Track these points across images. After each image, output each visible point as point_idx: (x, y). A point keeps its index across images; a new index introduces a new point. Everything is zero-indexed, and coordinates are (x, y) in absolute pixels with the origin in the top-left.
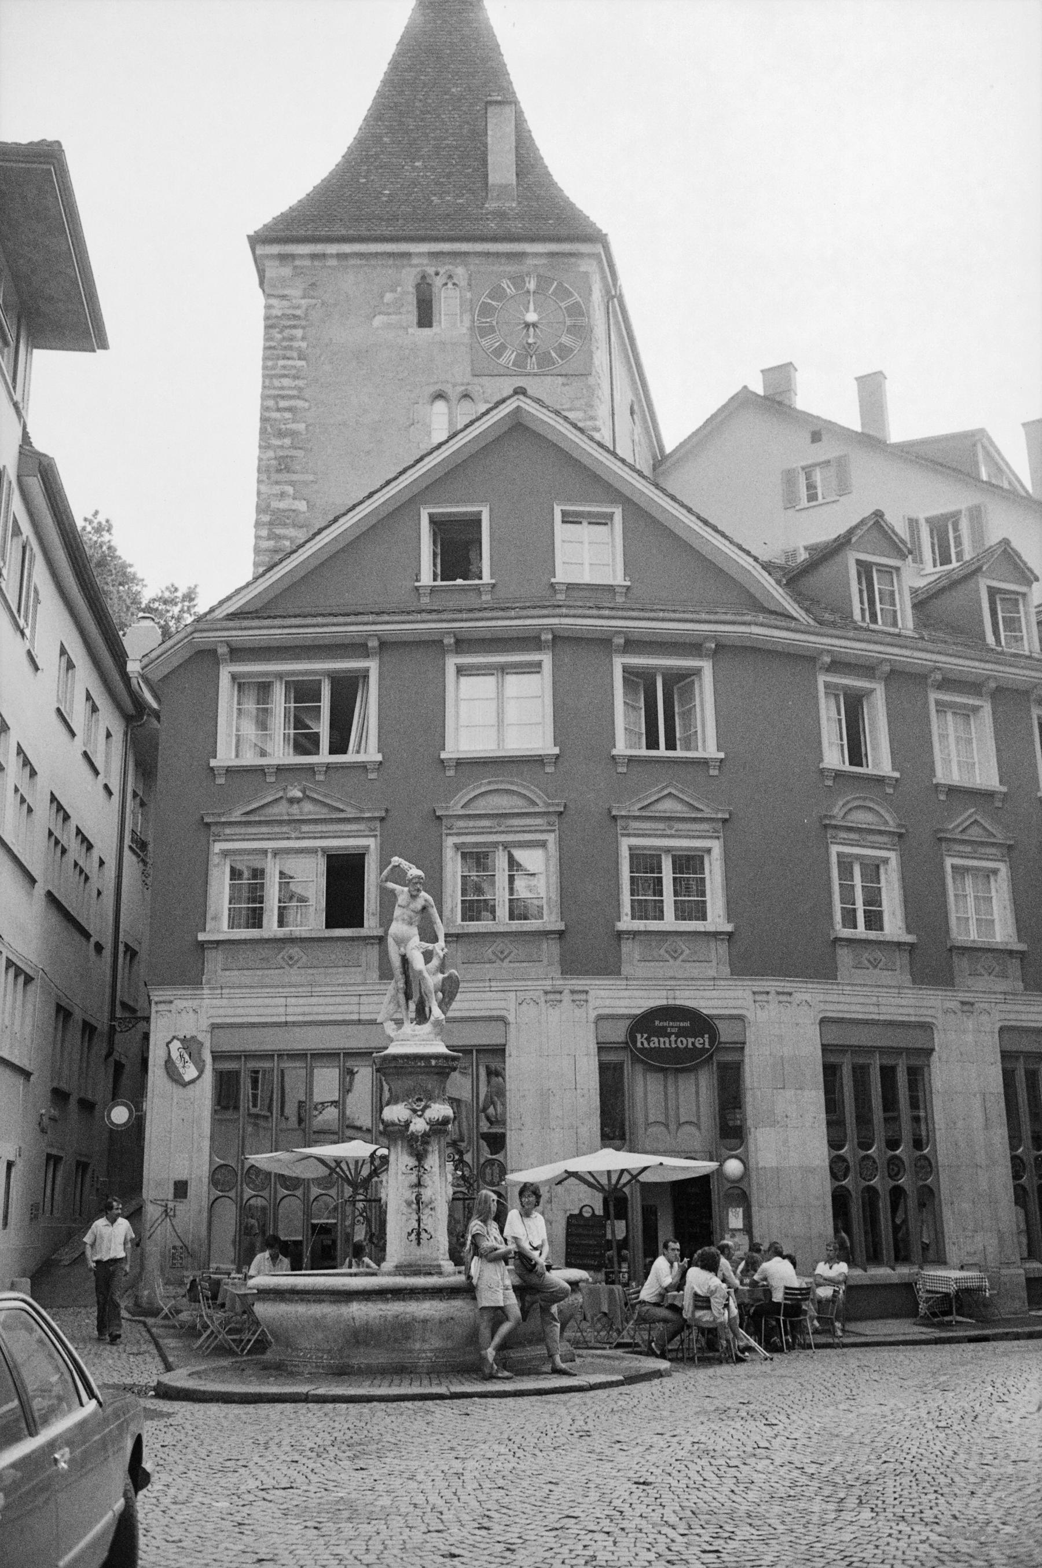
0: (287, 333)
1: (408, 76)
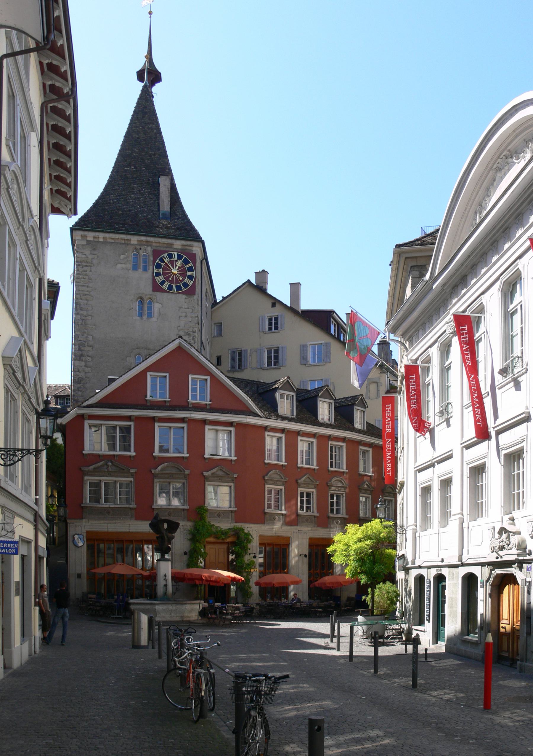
0: (85, 268)
1: (128, 152)
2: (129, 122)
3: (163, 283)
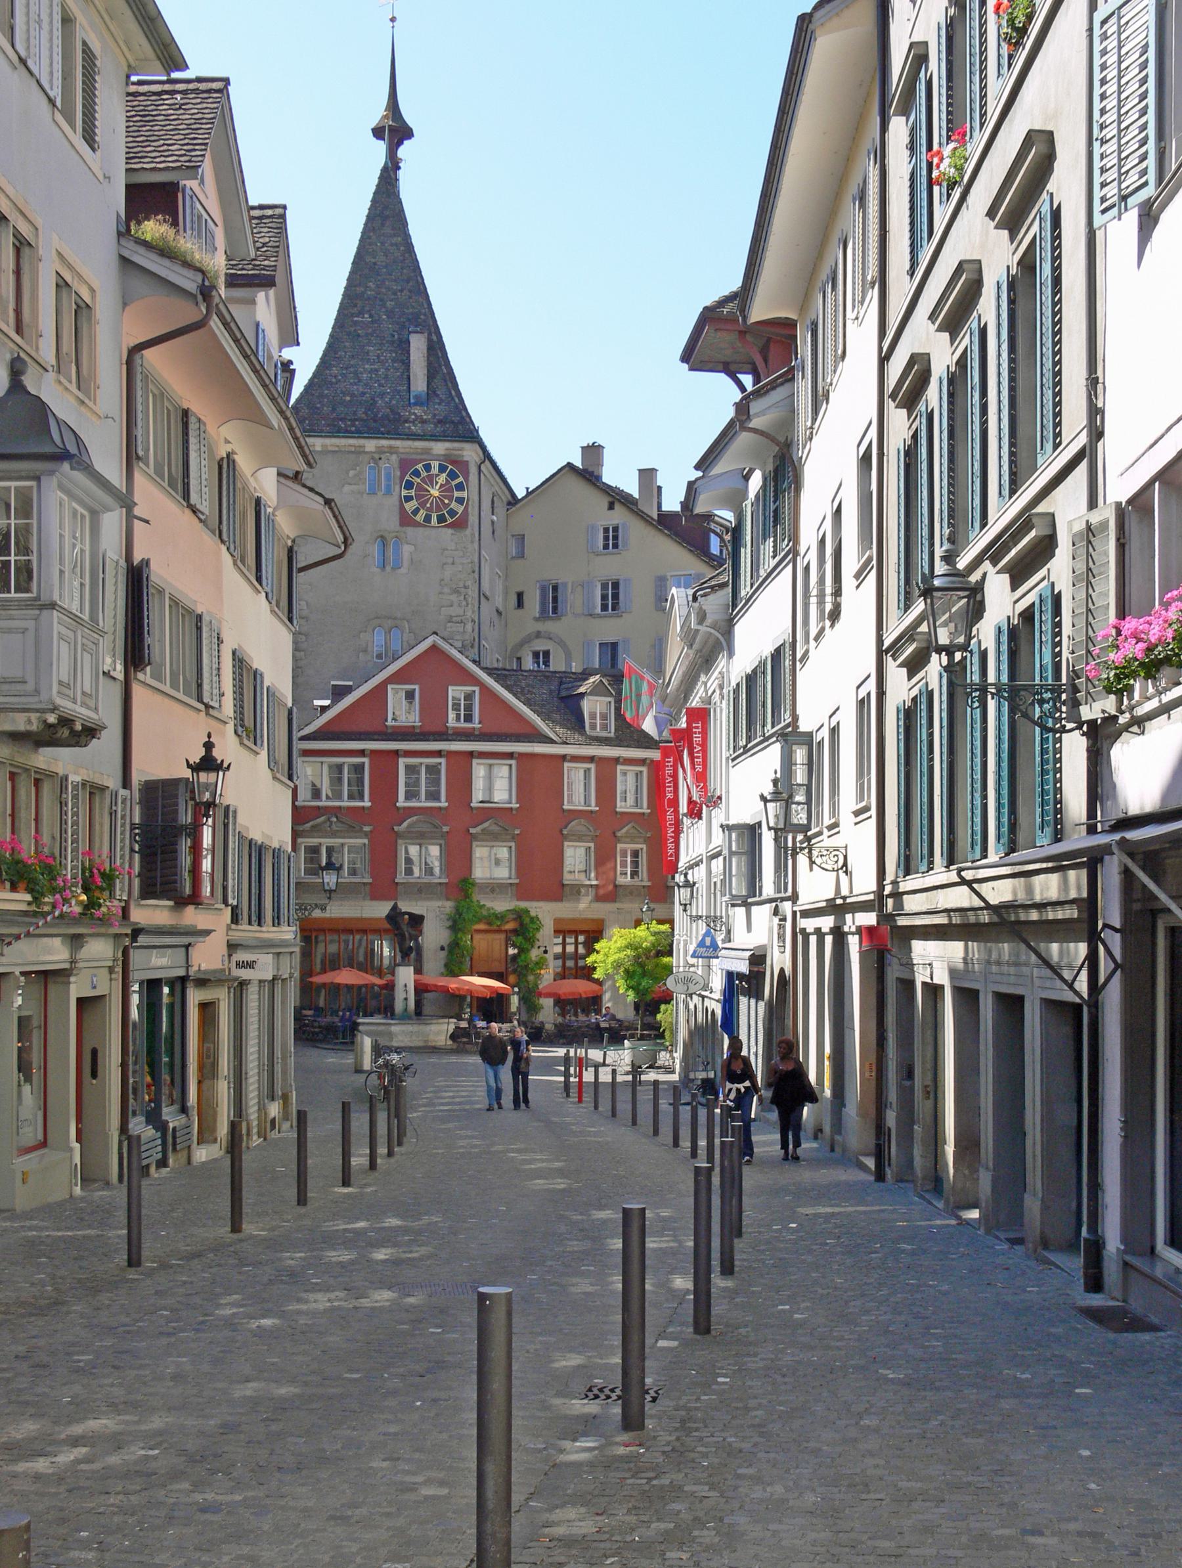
2: (366, 212)
3: (416, 512)
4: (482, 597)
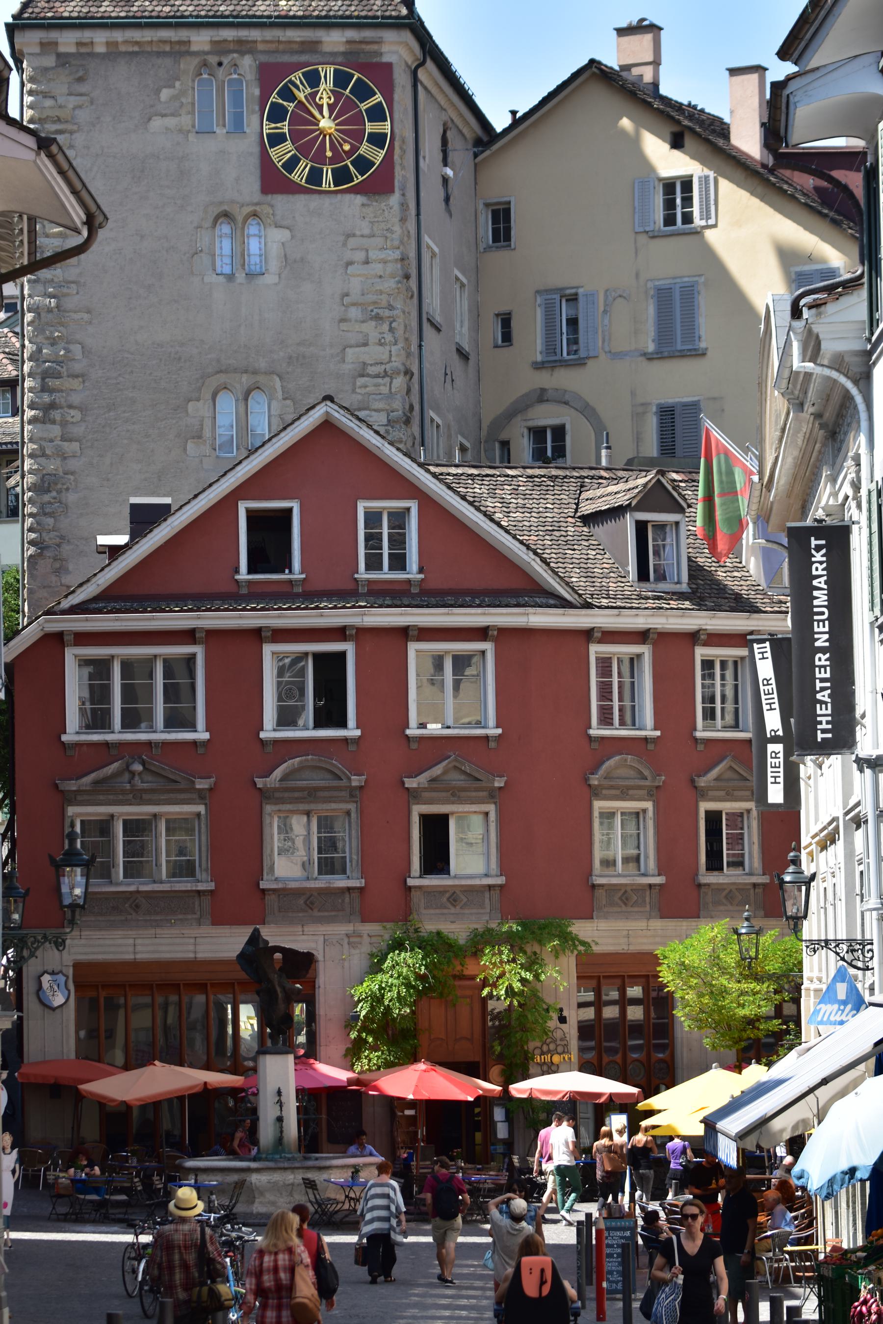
3: (291, 164)
4: (426, 326)
